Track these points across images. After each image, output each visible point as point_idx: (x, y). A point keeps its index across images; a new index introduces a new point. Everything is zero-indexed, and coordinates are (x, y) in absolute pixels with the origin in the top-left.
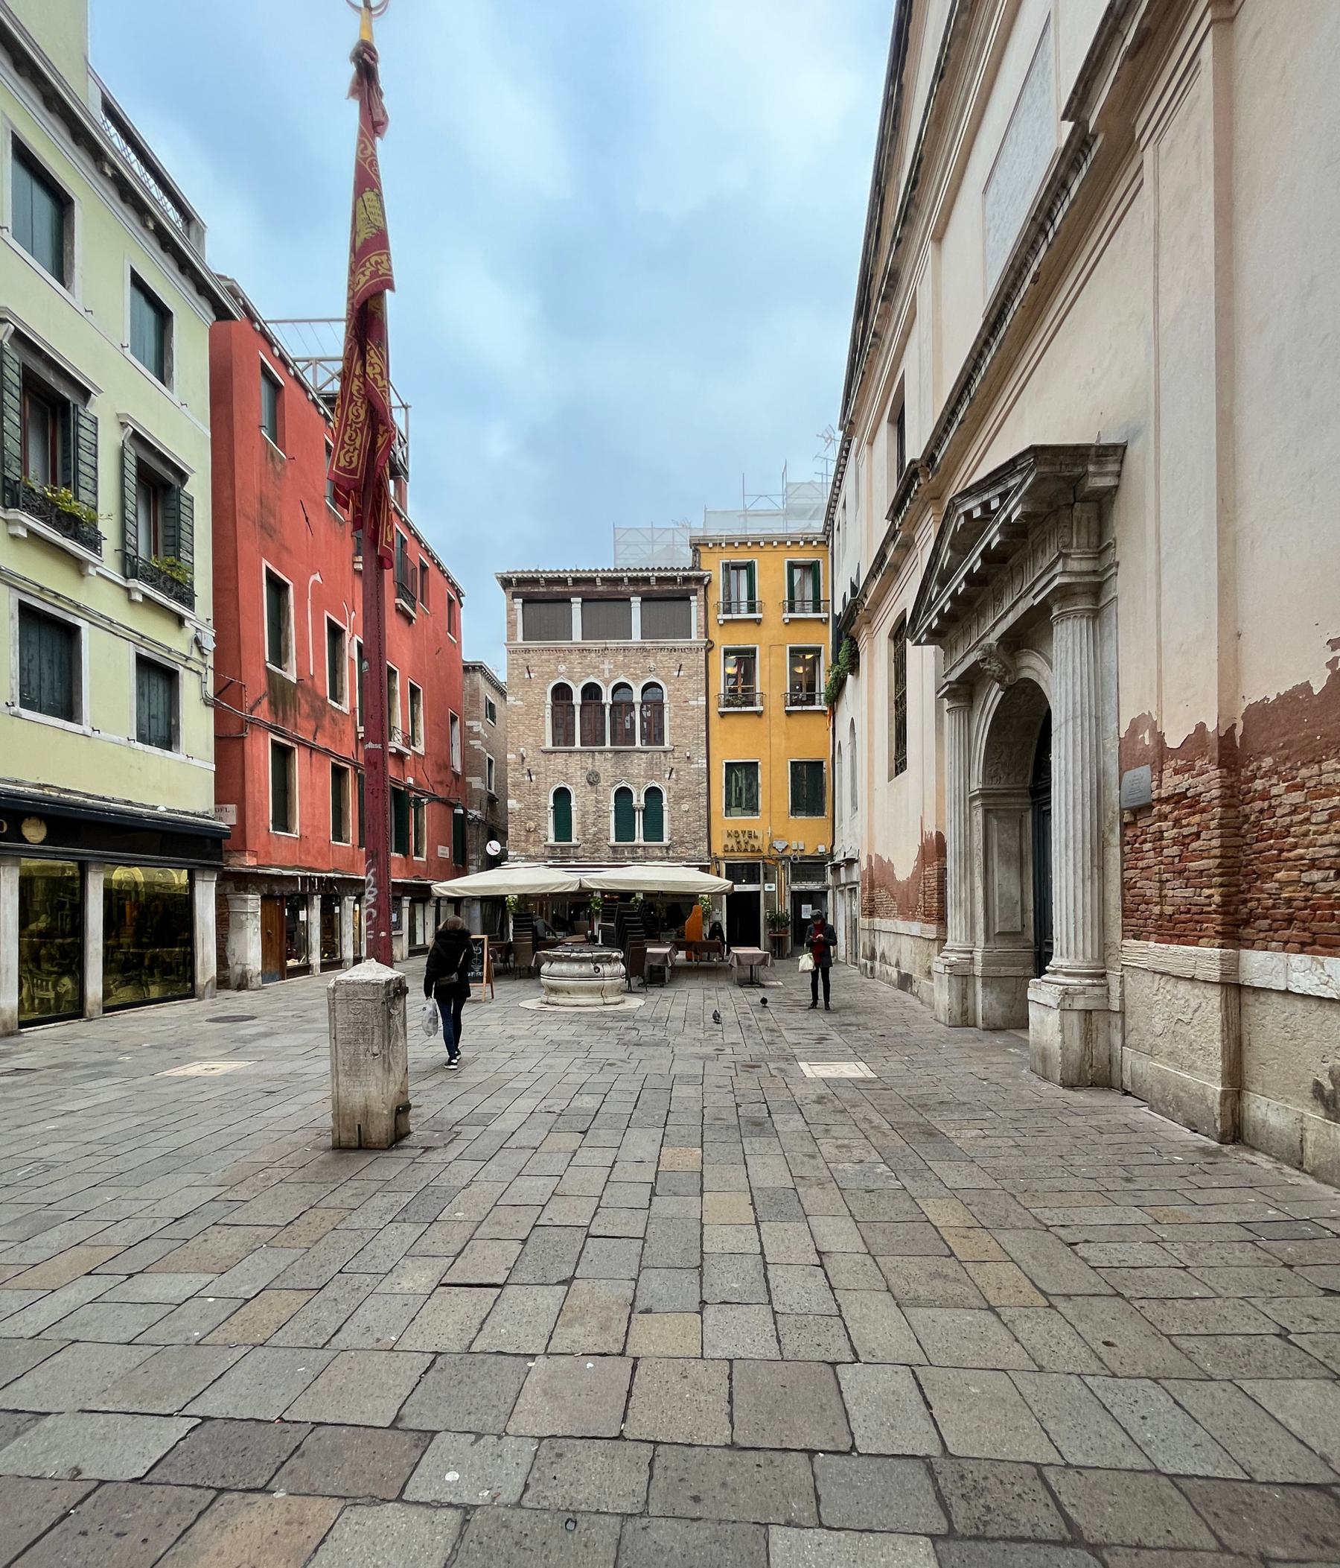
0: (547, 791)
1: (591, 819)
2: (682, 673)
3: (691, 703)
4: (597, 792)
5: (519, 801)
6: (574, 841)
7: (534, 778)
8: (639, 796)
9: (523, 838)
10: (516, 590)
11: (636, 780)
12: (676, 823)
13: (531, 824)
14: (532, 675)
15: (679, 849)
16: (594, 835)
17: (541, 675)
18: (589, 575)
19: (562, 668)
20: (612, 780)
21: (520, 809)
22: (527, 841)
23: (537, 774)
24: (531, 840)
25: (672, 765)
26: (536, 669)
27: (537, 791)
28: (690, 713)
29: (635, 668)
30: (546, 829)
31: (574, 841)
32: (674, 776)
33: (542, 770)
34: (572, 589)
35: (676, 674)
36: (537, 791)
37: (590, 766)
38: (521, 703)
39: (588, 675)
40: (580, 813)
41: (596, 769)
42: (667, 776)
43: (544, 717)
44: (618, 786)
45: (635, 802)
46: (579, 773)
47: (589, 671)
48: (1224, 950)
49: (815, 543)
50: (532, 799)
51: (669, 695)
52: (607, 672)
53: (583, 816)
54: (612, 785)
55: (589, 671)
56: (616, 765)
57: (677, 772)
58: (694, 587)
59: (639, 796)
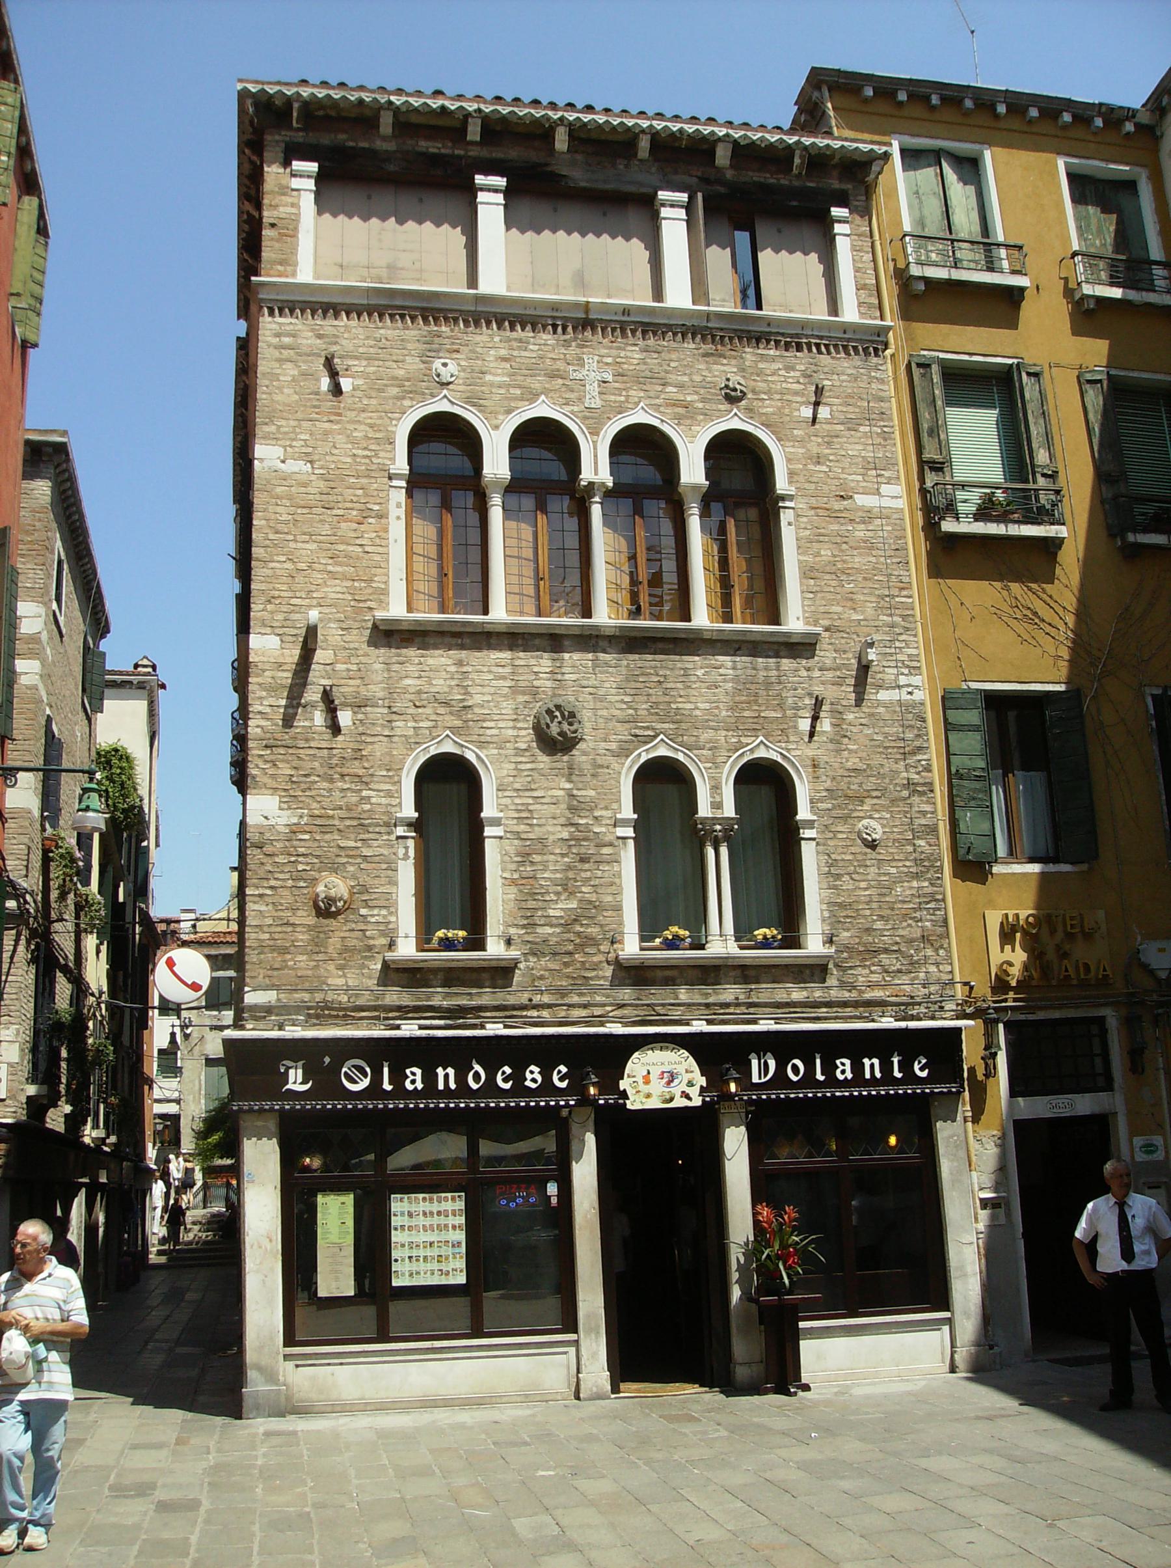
0: (394, 769)
1: (551, 870)
2: (824, 412)
3: (861, 500)
4: (570, 773)
5: (290, 801)
6: (495, 948)
7: (345, 718)
8: (716, 788)
9: (302, 937)
10: (300, 137)
11: (706, 735)
12: (846, 883)
13: (336, 886)
14: (346, 384)
15: (861, 975)
16: (567, 926)
17: (376, 387)
18: (538, 113)
19: (446, 367)
20: (623, 732)
21: (294, 830)
22: (317, 945)
23: (359, 705)
24: (334, 943)
25: (818, 690)
26: (358, 366)
27: (356, 768)
28: (860, 532)
29: (681, 386)
30: (390, 905)
31: (495, 948)
32: (825, 725)
33: (377, 691)
34: (474, 152)
35: (807, 412)
36: (356, 768)
37: (546, 684)
38: (302, 467)
39: (532, 396)
40: (512, 846)
41: (568, 699)
42: (805, 725)
43: (383, 516)
44: (644, 755)
45: (704, 810)
46: (507, 707)
47: (536, 383)
48: (1052, 868)
49: (1129, 127)
50: (339, 794)
51: (791, 474)
52: (593, 389)
53: (525, 856)
54: (623, 752)
55: (536, 383)
56: (631, 684)
57: (837, 714)
58: (836, 184)
59: (716, 788)
